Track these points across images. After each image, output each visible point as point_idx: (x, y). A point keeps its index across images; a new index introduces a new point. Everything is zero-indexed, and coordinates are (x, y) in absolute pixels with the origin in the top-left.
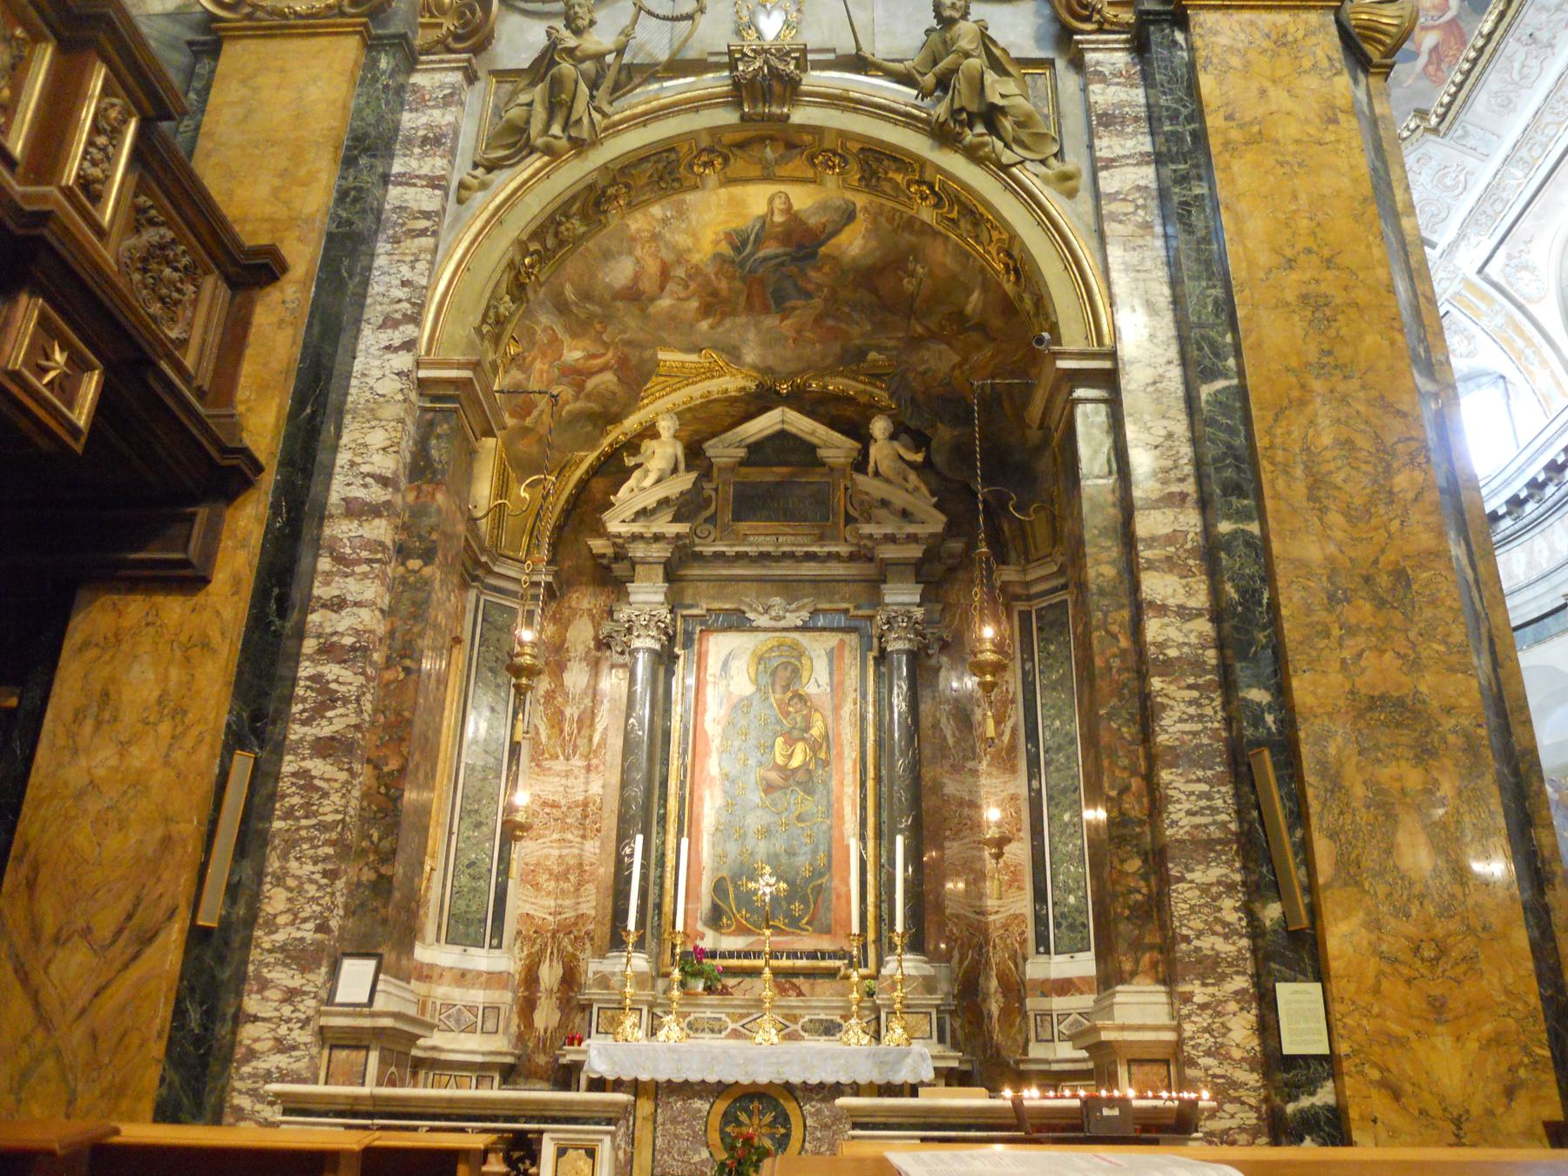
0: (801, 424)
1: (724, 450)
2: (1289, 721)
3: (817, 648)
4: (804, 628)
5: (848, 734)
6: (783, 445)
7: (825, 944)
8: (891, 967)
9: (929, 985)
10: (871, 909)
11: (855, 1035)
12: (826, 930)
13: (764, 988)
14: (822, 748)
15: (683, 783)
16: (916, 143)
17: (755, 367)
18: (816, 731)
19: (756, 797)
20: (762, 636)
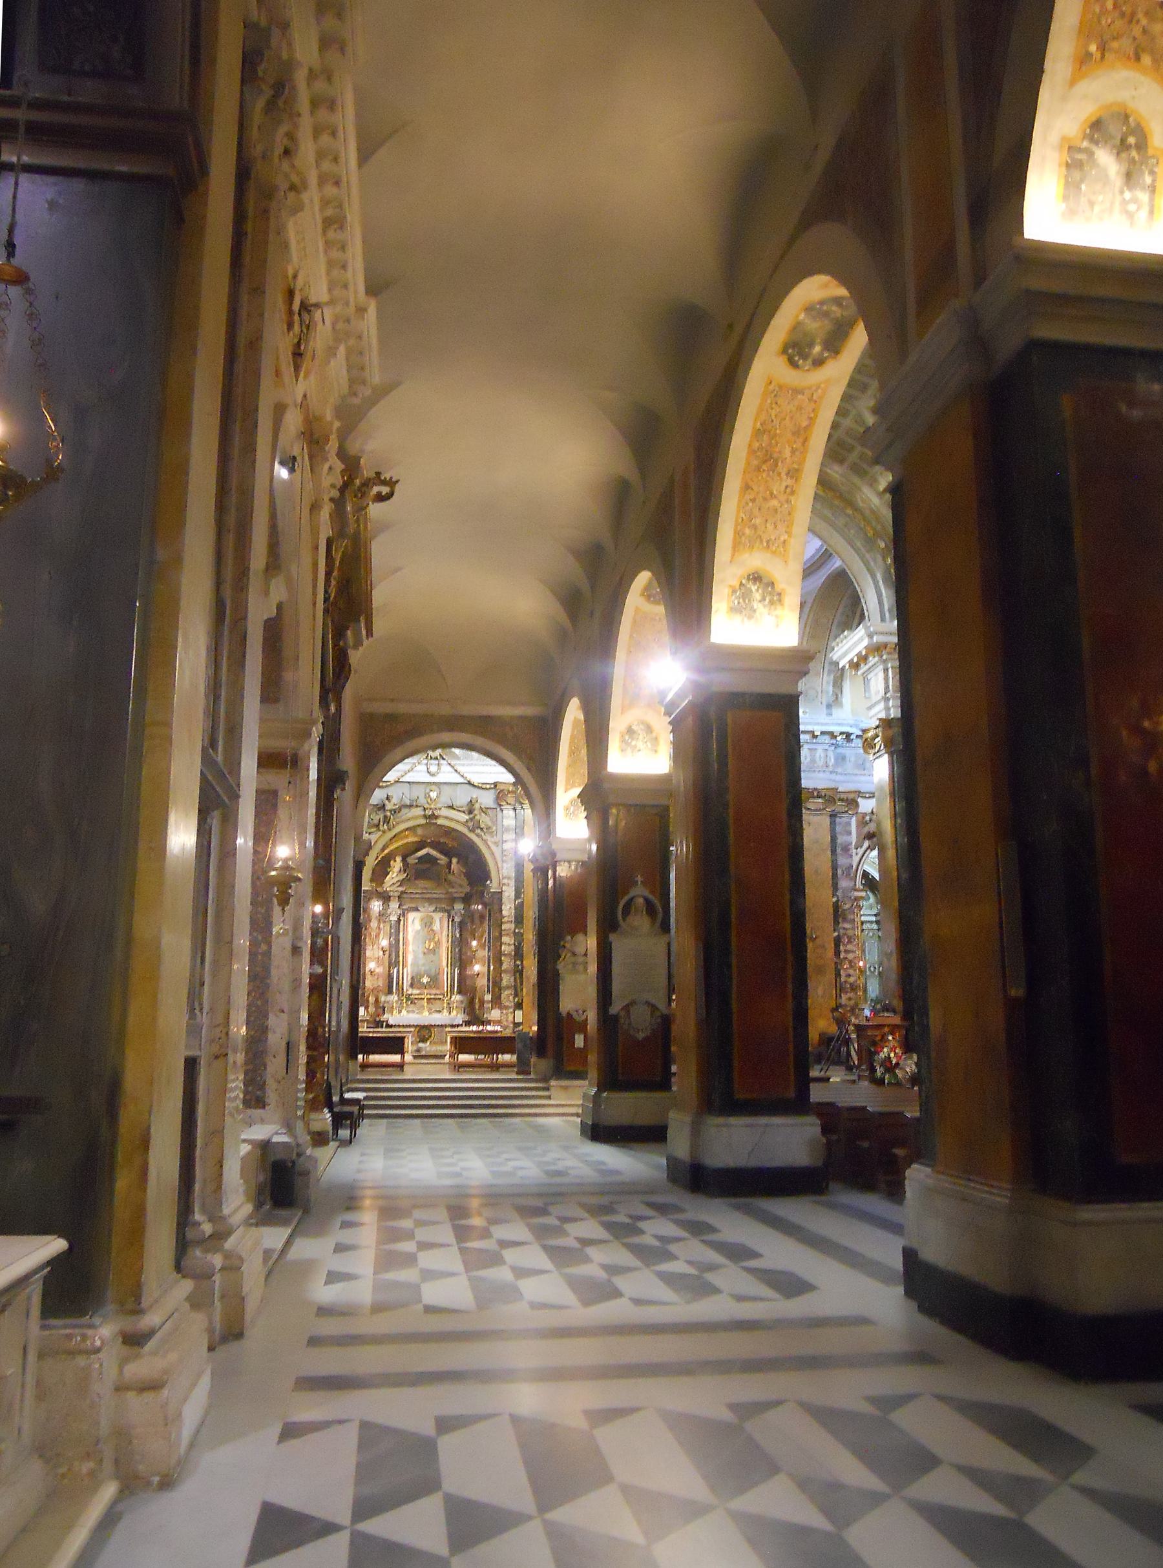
0: (434, 853)
1: (412, 860)
2: (522, 968)
3: (437, 916)
4: (434, 911)
5: (444, 940)
6: (428, 858)
7: (438, 992)
8: (453, 997)
9: (462, 1002)
10: (449, 984)
11: (445, 1012)
12: (438, 988)
13: (425, 1003)
14: (438, 943)
15: (403, 953)
16: (465, 830)
17: (420, 835)
18: (436, 939)
19: (421, 955)
20: (422, 914)
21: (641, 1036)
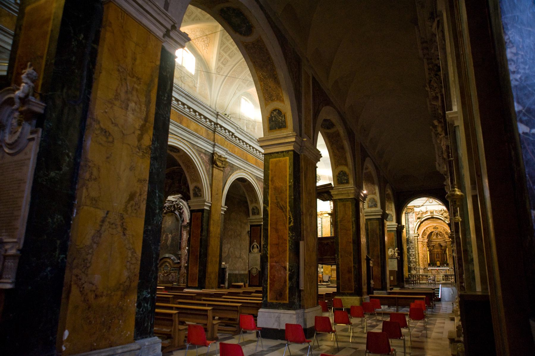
21: (254, 275)
